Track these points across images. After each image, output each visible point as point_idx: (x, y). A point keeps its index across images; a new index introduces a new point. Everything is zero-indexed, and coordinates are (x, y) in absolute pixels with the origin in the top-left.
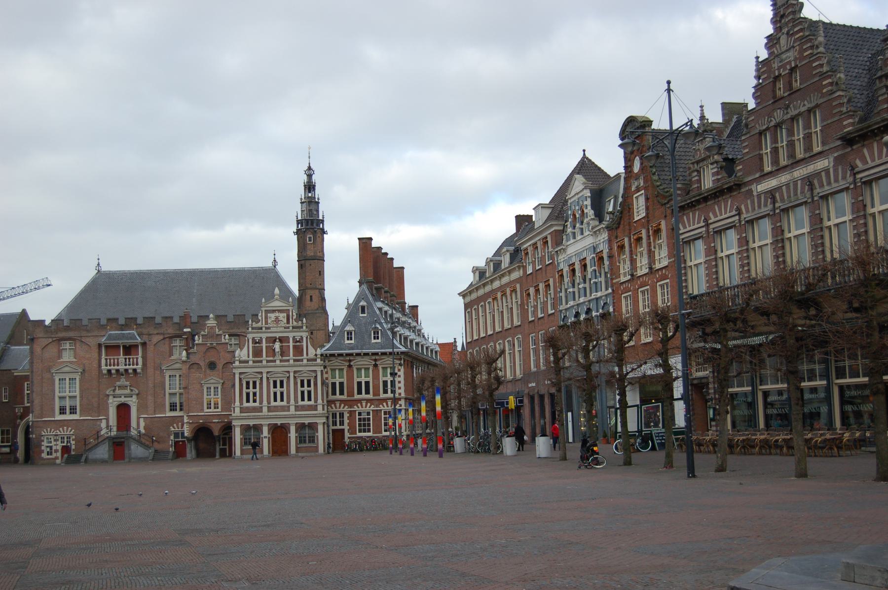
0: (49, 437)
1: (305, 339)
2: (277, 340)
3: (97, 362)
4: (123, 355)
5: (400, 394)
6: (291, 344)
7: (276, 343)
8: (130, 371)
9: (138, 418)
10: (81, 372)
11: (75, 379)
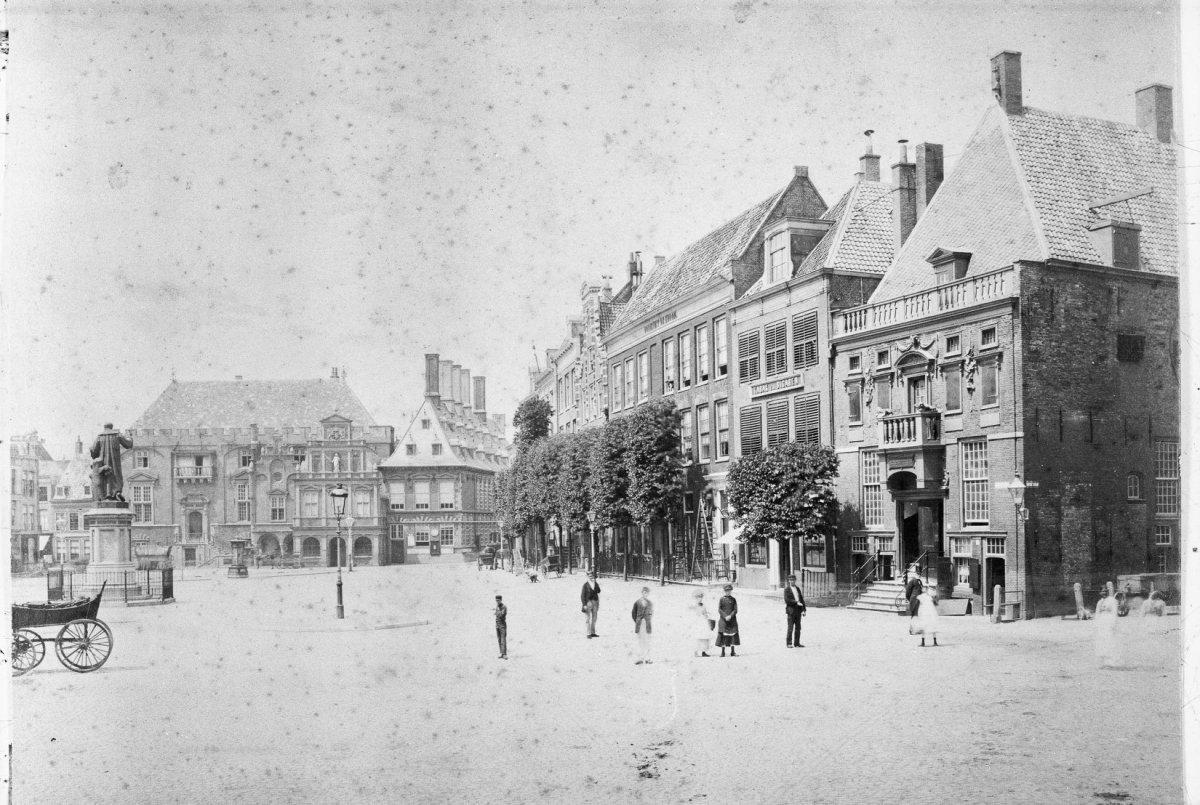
8: (201, 481)
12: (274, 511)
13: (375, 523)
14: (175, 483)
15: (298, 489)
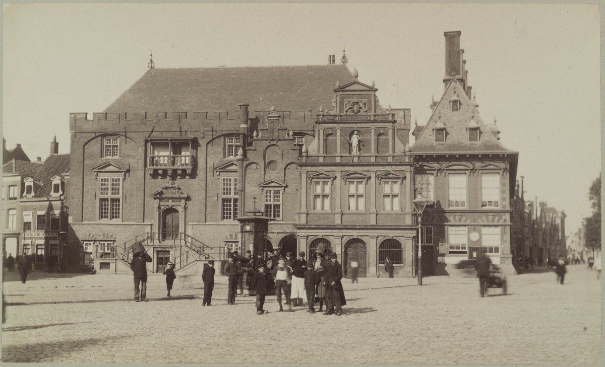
1: (390, 131)
2: (356, 132)
3: (142, 161)
5: (504, 206)
6: (373, 138)
10: (125, 172)
11: (119, 180)
13: (408, 221)
14: (148, 177)
15: (304, 176)
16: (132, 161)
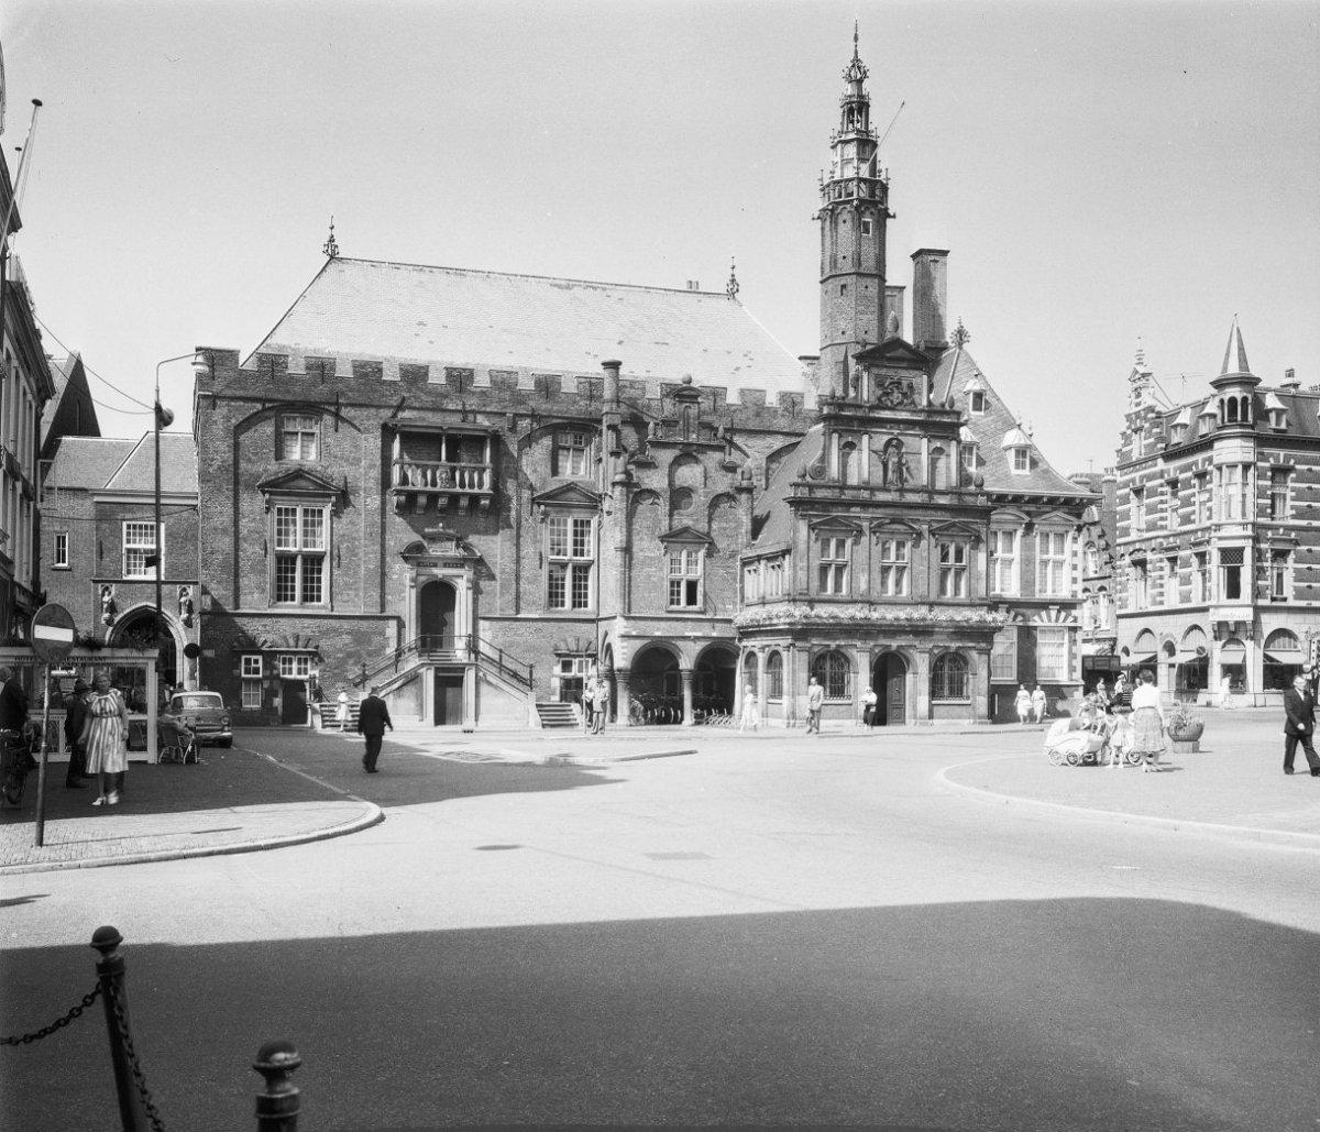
0: (253, 657)
2: (895, 442)
3: (376, 473)
4: (448, 459)
7: (891, 450)
9: (476, 619)
12: (675, 584)
16: (349, 471)
